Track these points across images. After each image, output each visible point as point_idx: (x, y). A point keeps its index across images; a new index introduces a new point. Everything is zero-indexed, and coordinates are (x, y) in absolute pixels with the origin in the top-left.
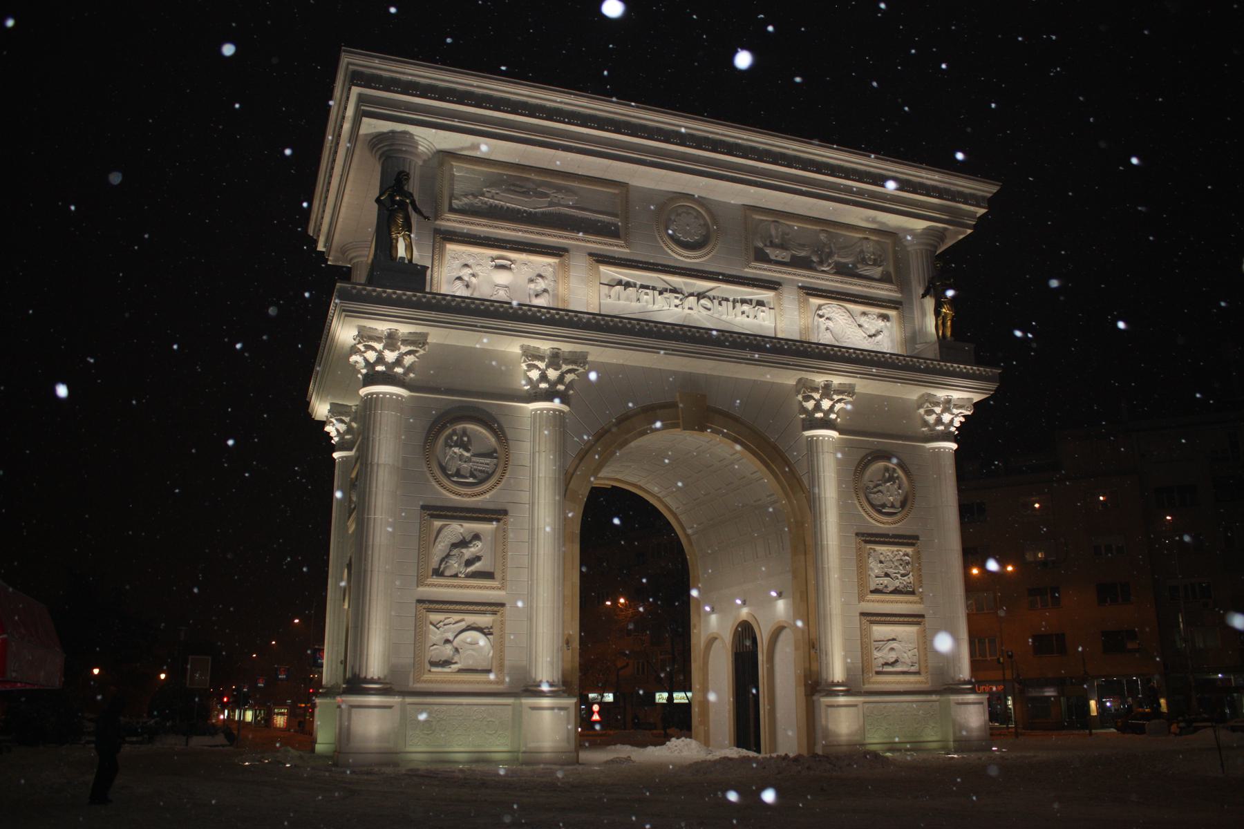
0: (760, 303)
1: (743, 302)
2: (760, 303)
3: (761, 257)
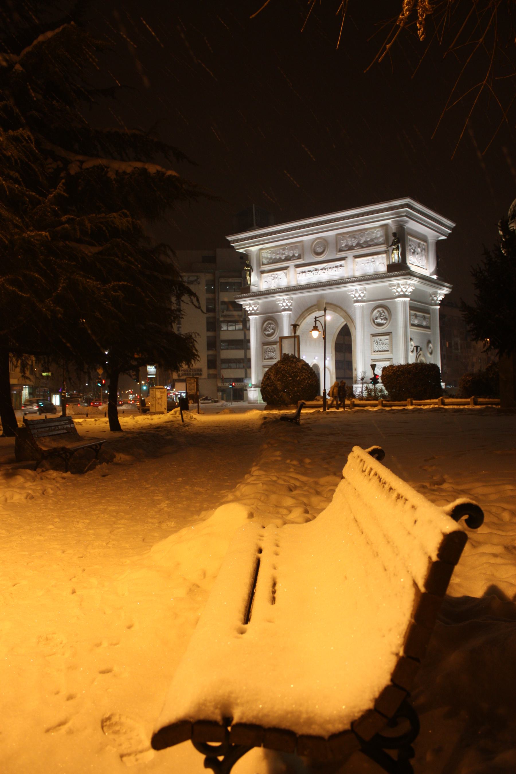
0: (341, 266)
1: (336, 267)
2: (341, 266)
3: (341, 251)
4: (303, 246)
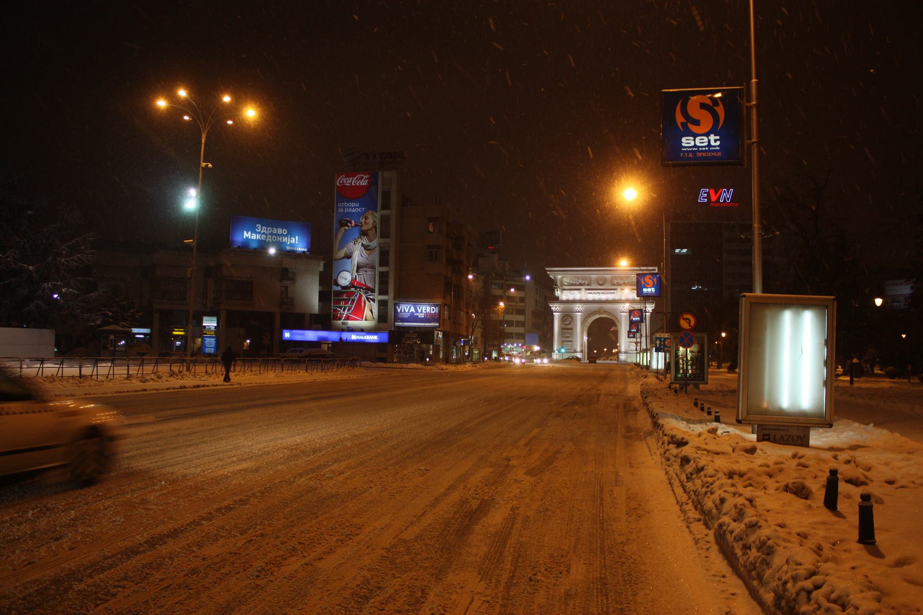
3: (614, 285)
4: (591, 281)
